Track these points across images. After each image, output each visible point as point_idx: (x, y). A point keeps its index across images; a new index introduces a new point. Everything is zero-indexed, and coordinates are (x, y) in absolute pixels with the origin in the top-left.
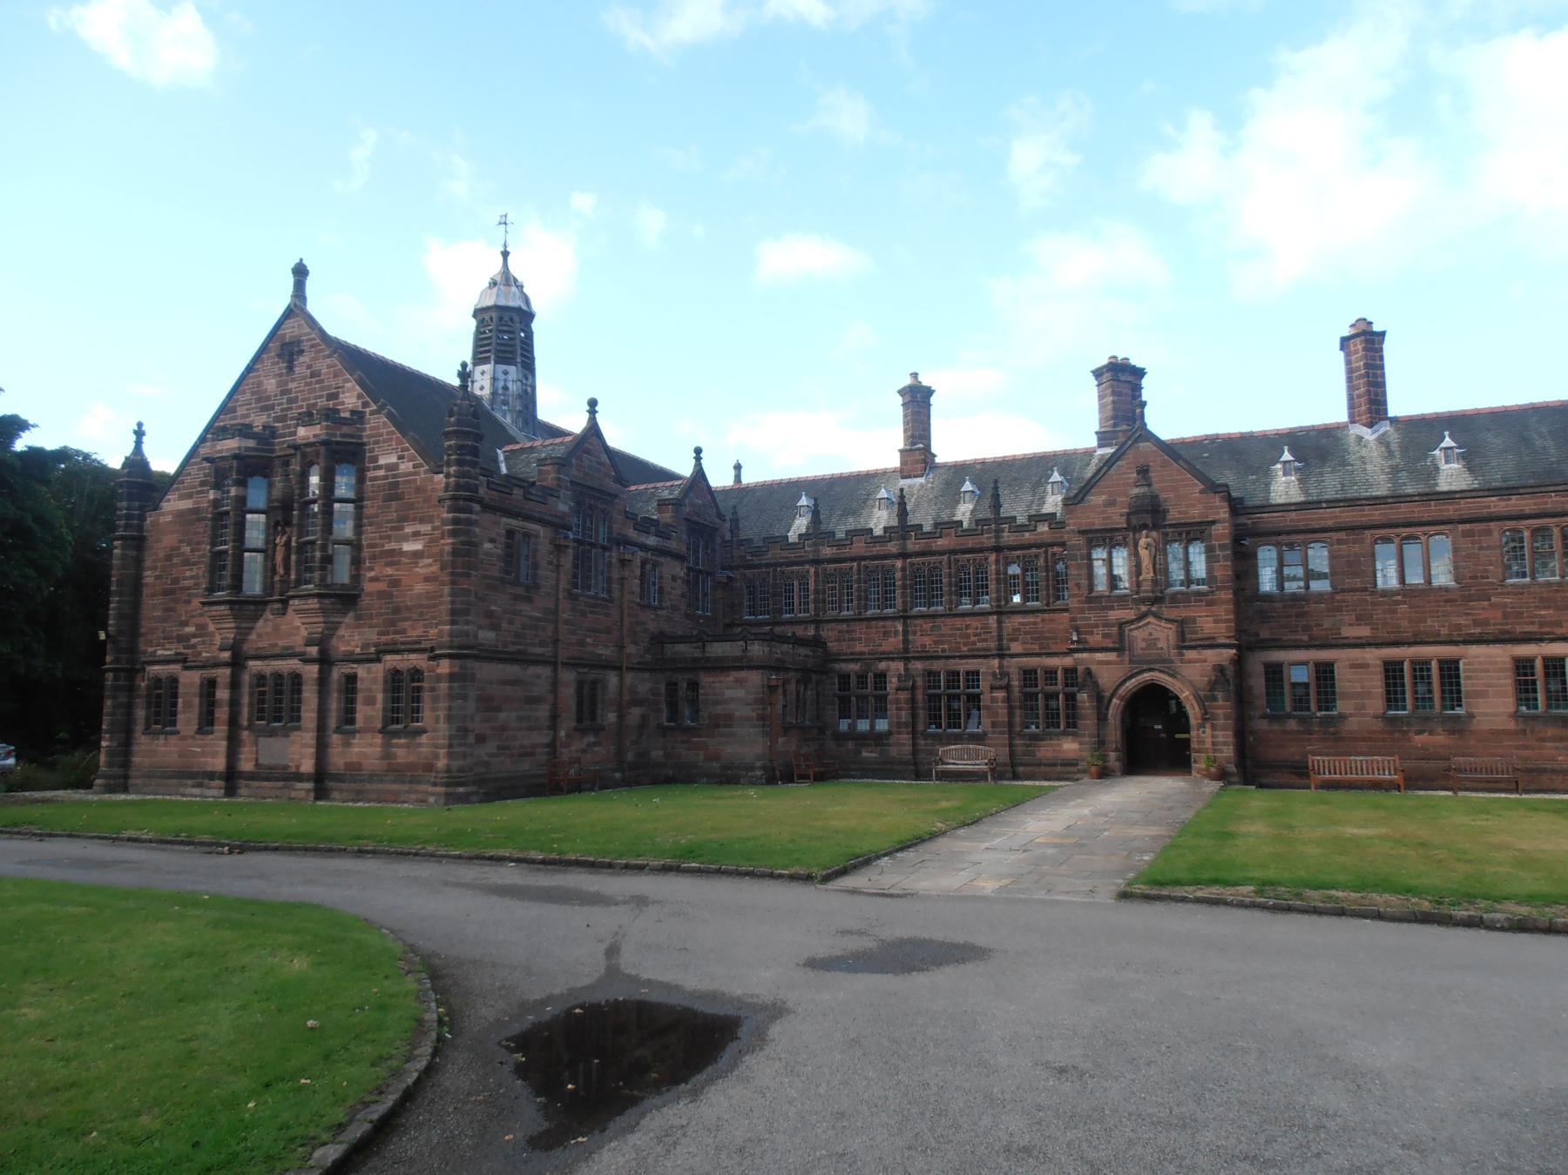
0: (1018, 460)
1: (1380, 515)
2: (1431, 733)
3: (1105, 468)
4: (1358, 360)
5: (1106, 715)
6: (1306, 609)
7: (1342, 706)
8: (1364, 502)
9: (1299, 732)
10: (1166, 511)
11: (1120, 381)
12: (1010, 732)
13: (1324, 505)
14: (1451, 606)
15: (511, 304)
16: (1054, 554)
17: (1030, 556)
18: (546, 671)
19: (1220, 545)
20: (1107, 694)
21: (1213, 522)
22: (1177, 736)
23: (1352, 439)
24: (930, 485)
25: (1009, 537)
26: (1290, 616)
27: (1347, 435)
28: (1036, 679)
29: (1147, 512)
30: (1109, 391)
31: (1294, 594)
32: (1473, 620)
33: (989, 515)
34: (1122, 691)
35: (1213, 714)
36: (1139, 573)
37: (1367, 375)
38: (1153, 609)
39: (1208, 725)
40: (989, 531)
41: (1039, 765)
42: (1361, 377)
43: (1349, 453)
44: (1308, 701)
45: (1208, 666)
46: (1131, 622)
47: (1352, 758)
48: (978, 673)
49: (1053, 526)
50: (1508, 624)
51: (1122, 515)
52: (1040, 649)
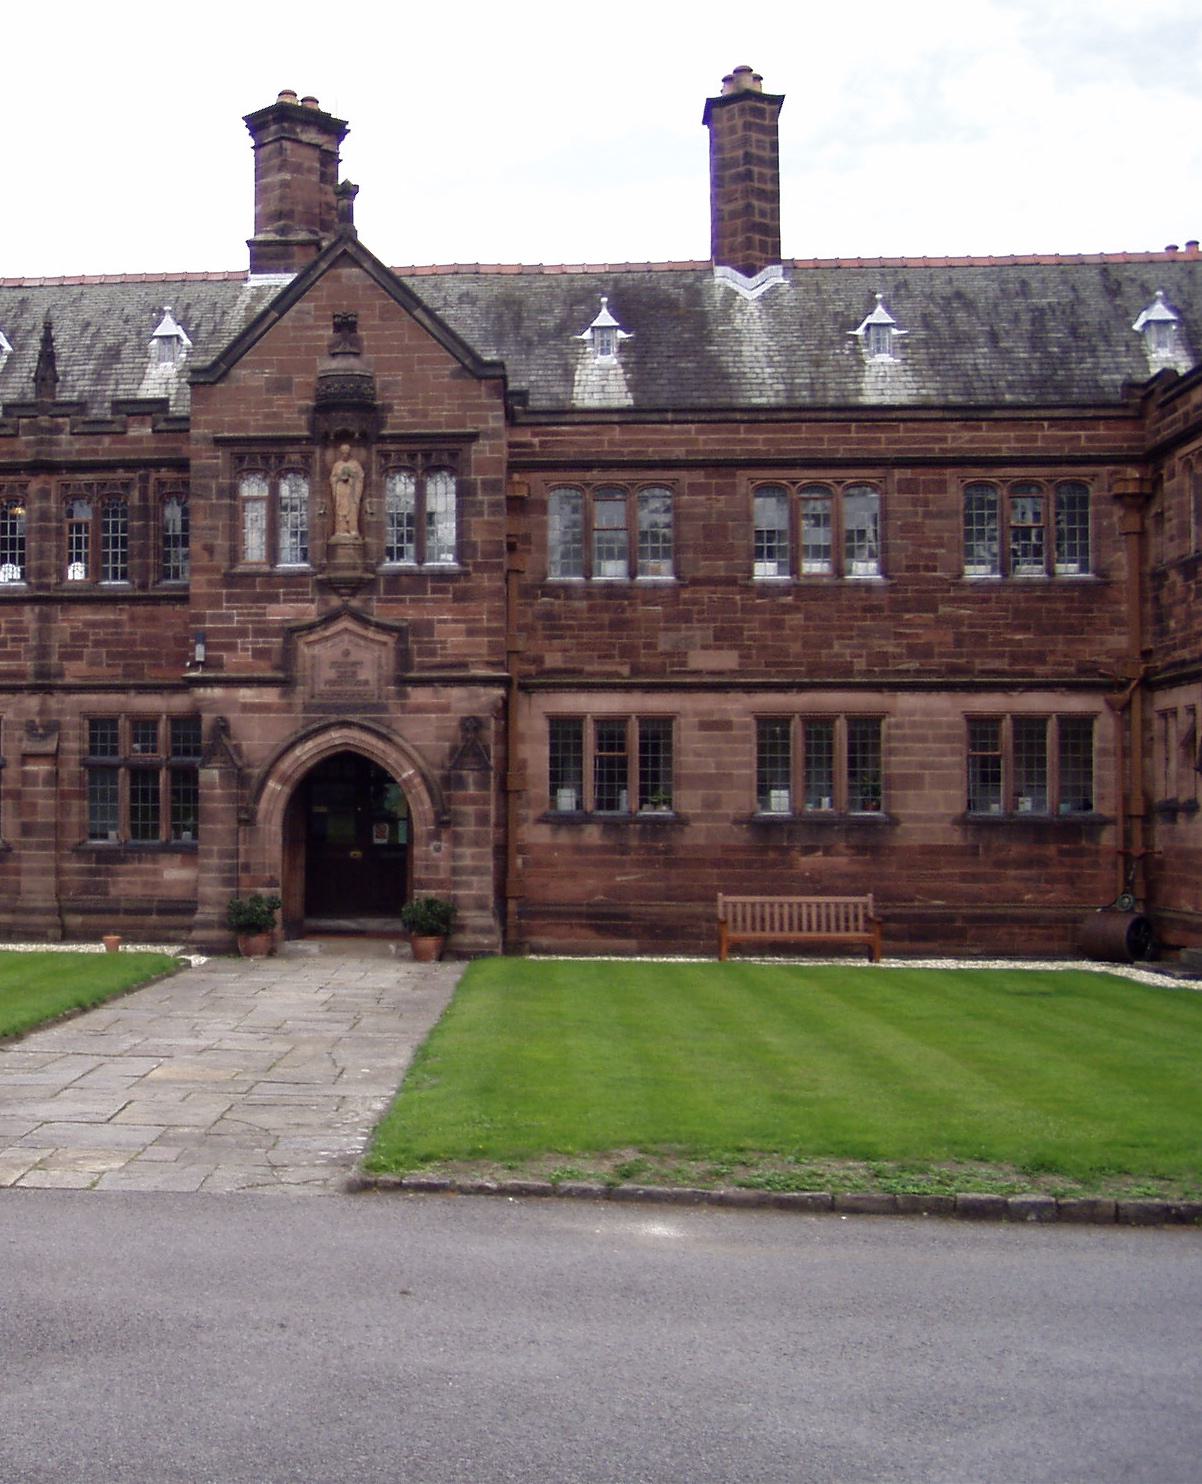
1: (766, 441)
2: (827, 851)
5: (253, 814)
6: (628, 615)
7: (688, 801)
9: (603, 849)
14: (873, 619)
16: (161, 484)
17: (115, 486)
19: (484, 483)
20: (256, 772)
25: (71, 443)
26: (601, 627)
28: (115, 738)
31: (609, 586)
32: (910, 647)
34: (286, 765)
35: (456, 813)
38: (355, 603)
45: (452, 721)
46: (311, 628)
49: (162, 426)
50: (961, 655)
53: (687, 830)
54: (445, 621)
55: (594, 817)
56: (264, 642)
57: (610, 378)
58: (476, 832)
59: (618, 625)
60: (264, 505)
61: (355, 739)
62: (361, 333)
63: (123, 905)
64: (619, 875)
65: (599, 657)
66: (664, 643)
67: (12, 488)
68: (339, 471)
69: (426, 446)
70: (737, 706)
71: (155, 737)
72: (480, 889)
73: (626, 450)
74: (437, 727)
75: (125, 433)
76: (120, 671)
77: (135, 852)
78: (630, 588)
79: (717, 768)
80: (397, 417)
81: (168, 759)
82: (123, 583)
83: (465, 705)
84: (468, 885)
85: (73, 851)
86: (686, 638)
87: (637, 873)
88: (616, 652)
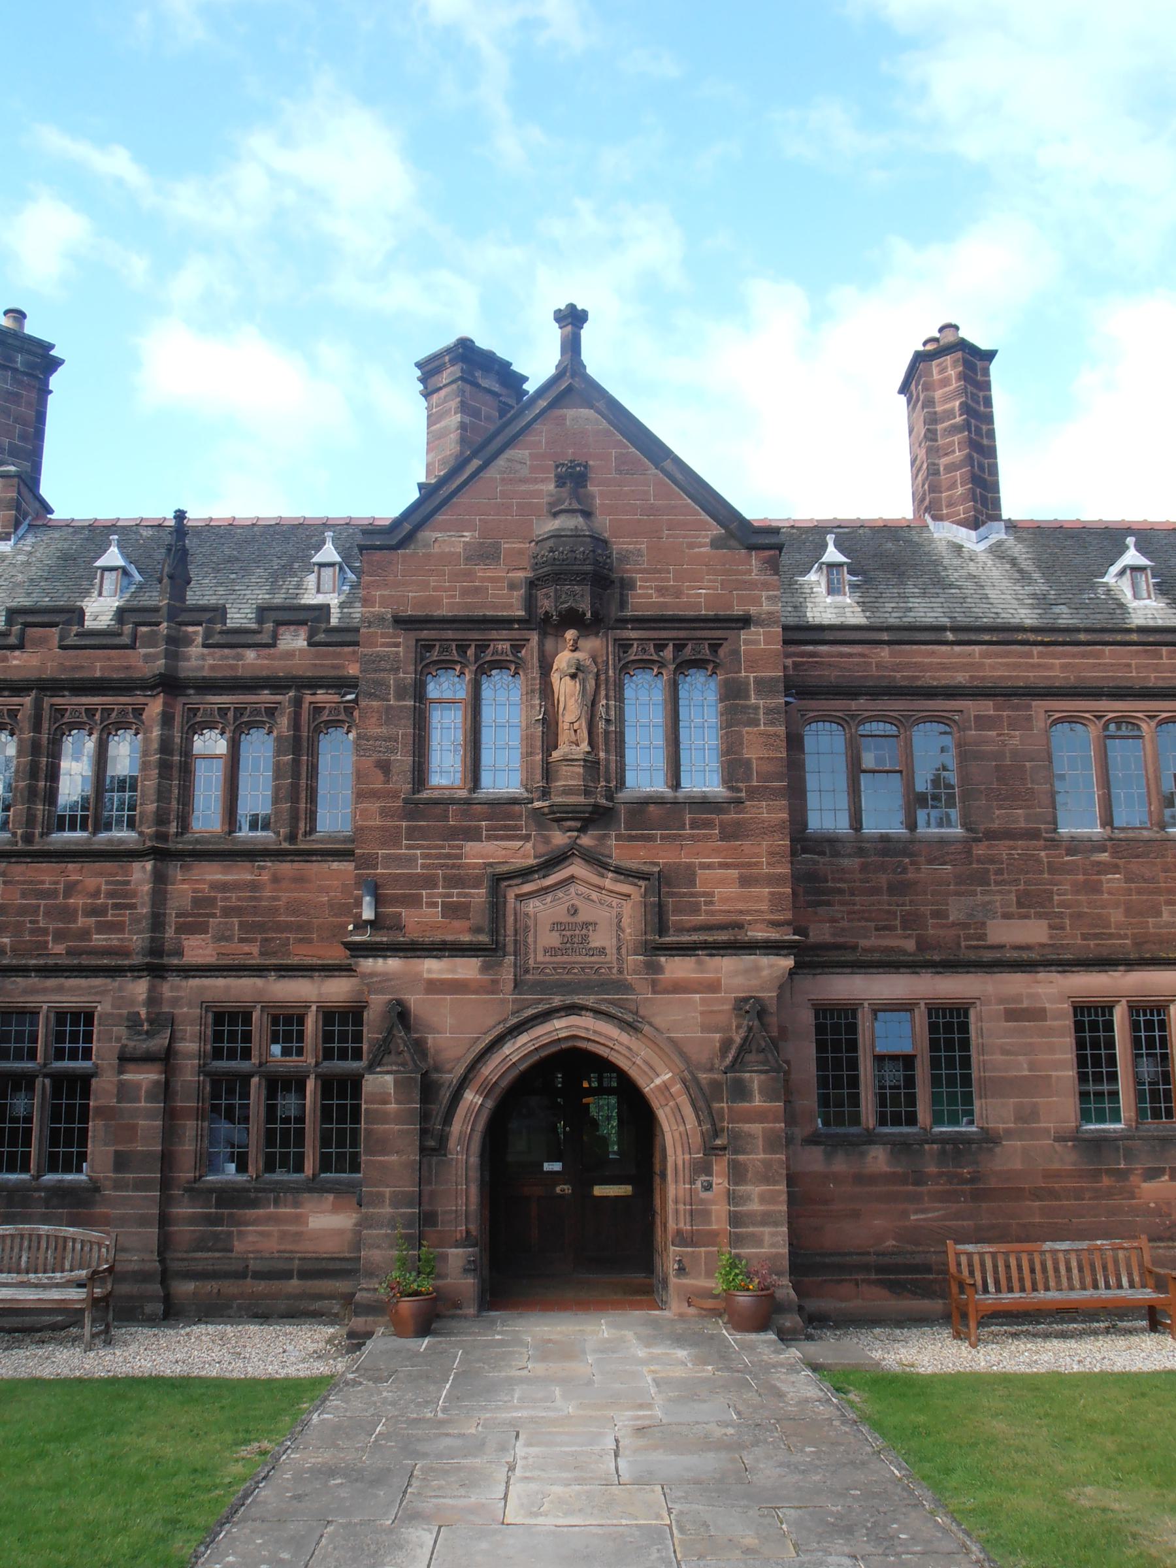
0: (243, 527)
1: (1064, 667)
3: (476, 463)
4: (947, 399)
5: (443, 1139)
6: (911, 875)
8: (1032, 637)
10: (627, 585)
11: (477, 385)
12: (165, 1184)
13: (950, 636)
16: (317, 710)
19: (758, 681)
20: (452, 1077)
21: (745, 621)
22: (599, 1191)
23: (942, 548)
24: (22, 558)
25: (203, 657)
27: (931, 541)
28: (247, 1037)
29: (580, 578)
30: (454, 404)
31: (885, 839)
33: (156, 598)
34: (491, 1069)
35: (735, 1136)
36: (550, 741)
37: (967, 426)
39: (720, 1166)
40: (151, 641)
41: (241, 1275)
42: (954, 429)
43: (946, 569)
44: (912, 1100)
45: (723, 1004)
46: (525, 874)
47: (1048, 1245)
48: (89, 1017)
49: (321, 637)
51: (512, 586)
52: (262, 954)
53: (998, 1150)
54: (709, 866)
55: (878, 1135)
56: (459, 895)
57: (848, 614)
58: (763, 1161)
59: (898, 888)
60: (460, 714)
61: (587, 1029)
62: (591, 488)
63: (253, 1265)
64: (916, 1212)
65: (877, 929)
66: (956, 911)
67: (123, 713)
68: (564, 665)
69: (682, 634)
70: (1052, 990)
71: (301, 1036)
72: (773, 1245)
73: (899, 675)
74: (702, 1013)
75: (274, 645)
76: (255, 949)
77: (272, 1191)
78: (912, 842)
79: (1030, 1070)
80: (641, 596)
81: (317, 1064)
82: (264, 834)
83: (739, 980)
84: (757, 1241)
85: (186, 1190)
86: (985, 904)
87: (938, 1210)
88: (898, 922)
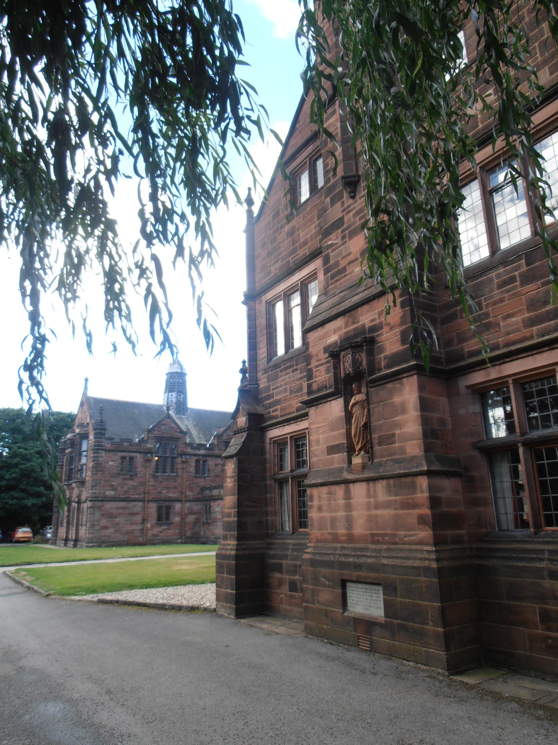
15: (174, 371)
18: (141, 504)
